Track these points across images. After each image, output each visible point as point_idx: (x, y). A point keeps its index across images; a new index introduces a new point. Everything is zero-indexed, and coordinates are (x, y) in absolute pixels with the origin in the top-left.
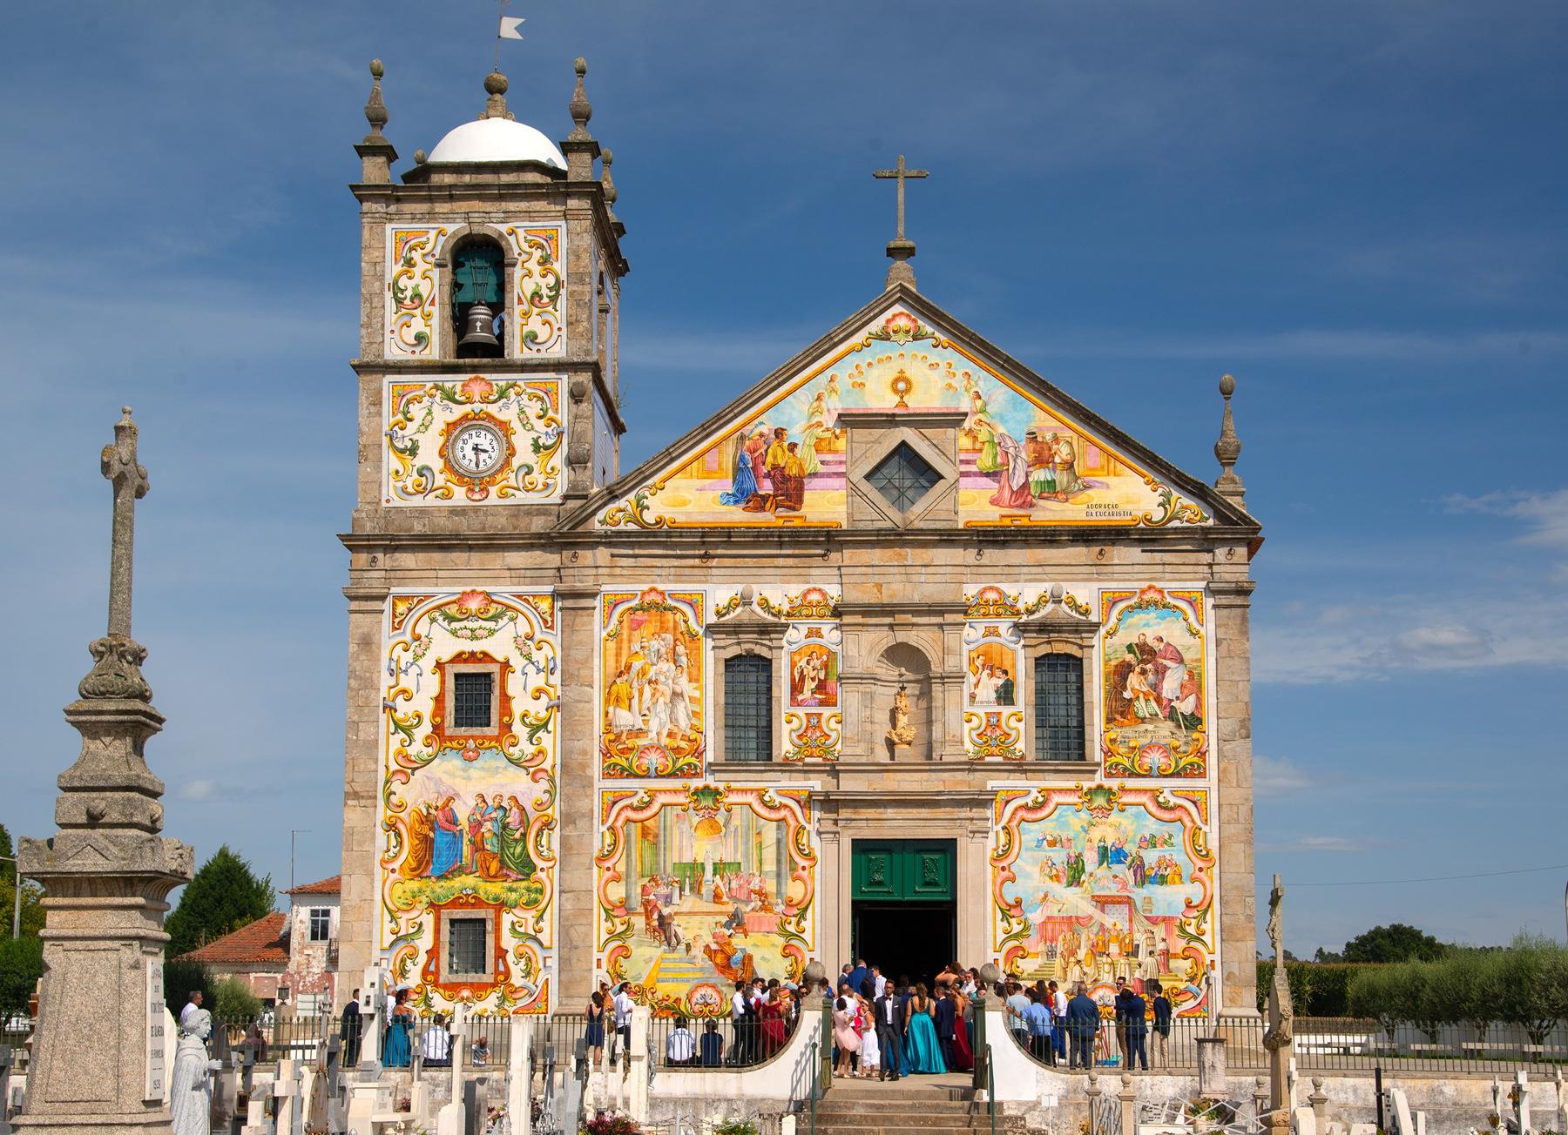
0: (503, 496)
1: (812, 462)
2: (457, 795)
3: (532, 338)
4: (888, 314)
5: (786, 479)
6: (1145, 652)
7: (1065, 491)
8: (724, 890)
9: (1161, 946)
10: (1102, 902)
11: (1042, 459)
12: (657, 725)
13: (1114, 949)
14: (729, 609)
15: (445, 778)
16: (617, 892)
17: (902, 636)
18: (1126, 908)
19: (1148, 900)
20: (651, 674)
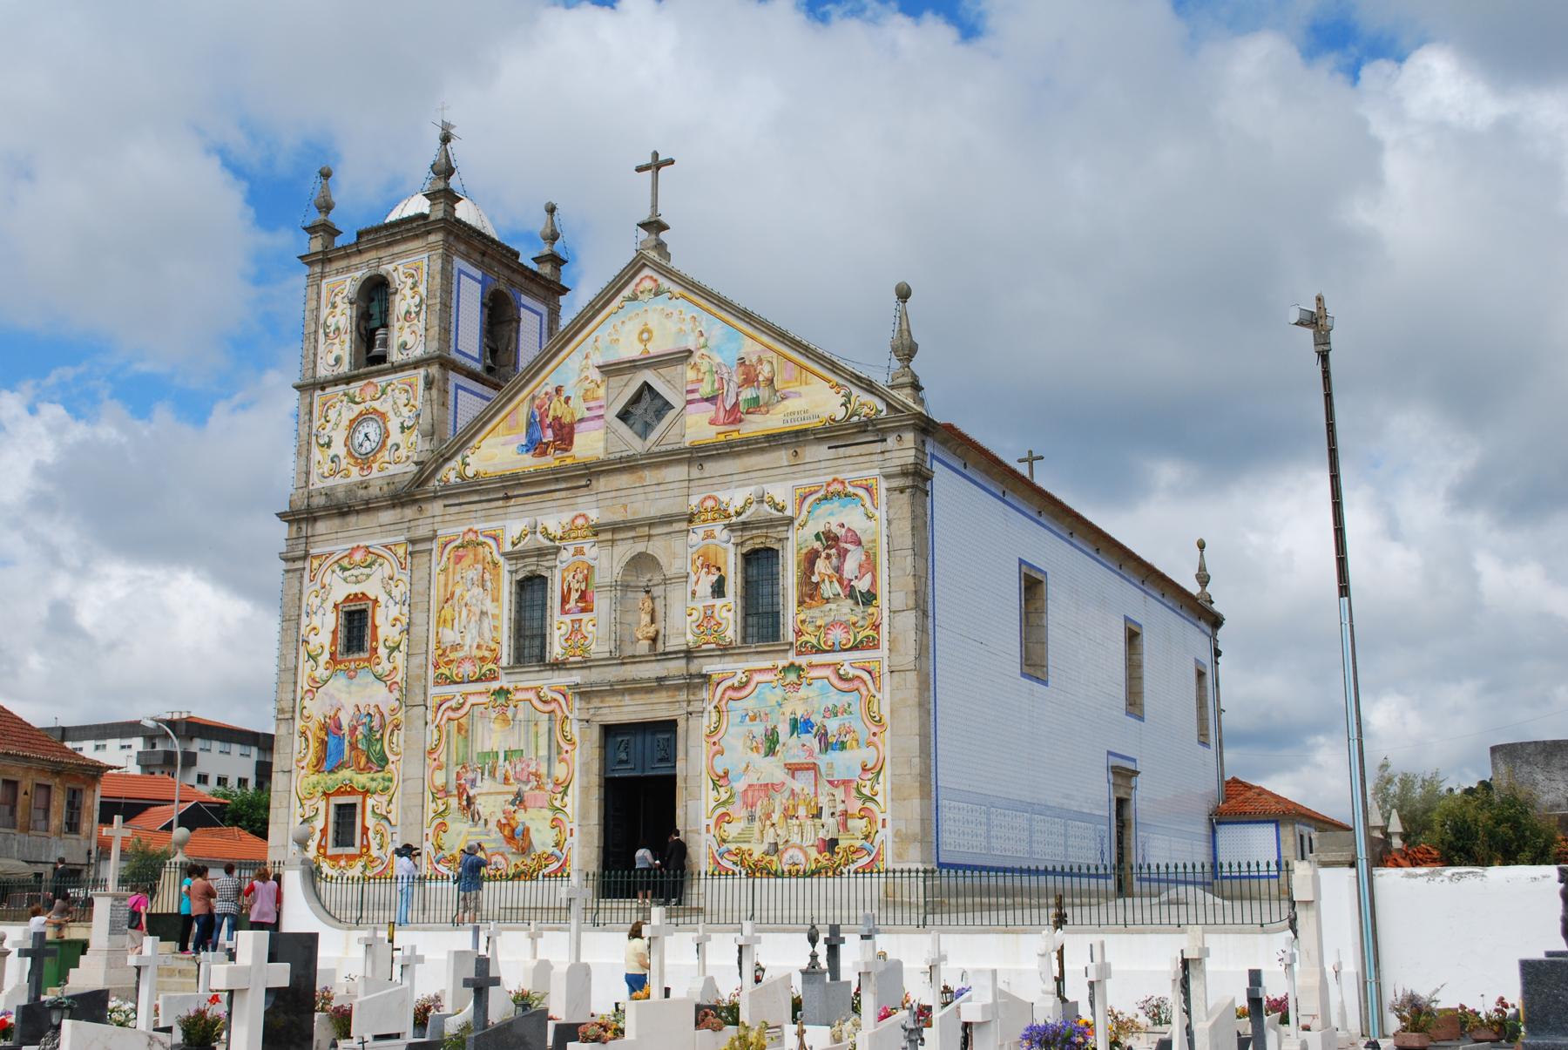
0: (381, 470)
1: (579, 408)
3: (404, 346)
4: (637, 280)
5: (562, 426)
6: (830, 539)
7: (766, 404)
8: (511, 773)
9: (841, 807)
10: (793, 769)
11: (750, 380)
12: (470, 640)
13: (802, 812)
14: (520, 539)
16: (440, 778)
17: (640, 547)
18: (812, 773)
19: (831, 766)
20: (467, 596)
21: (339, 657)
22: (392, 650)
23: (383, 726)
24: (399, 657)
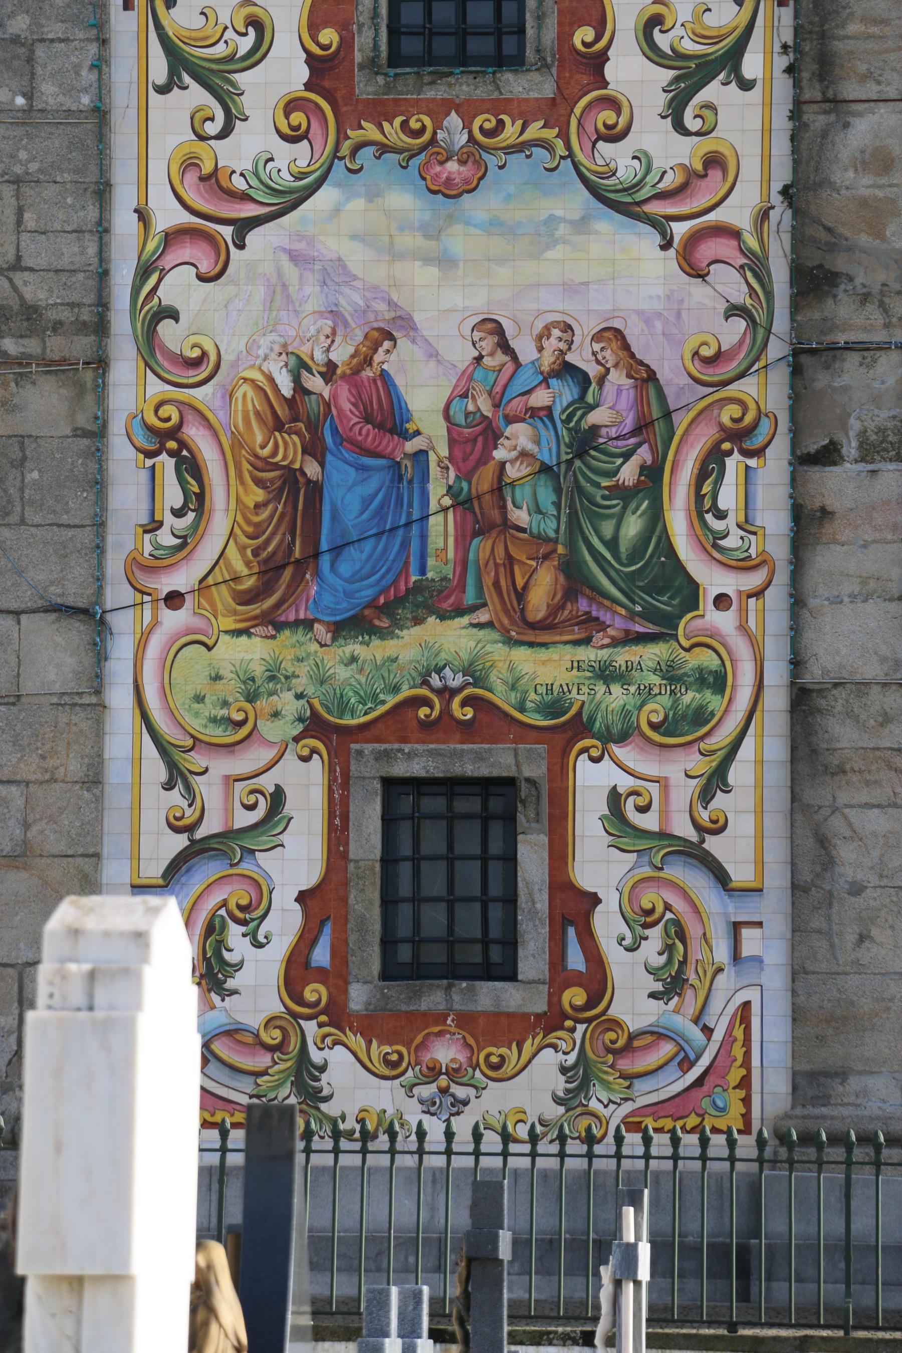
2: (406, 322)
15: (357, 257)
21: (365, 88)
22: (691, 75)
23: (653, 422)
24: (747, 118)
